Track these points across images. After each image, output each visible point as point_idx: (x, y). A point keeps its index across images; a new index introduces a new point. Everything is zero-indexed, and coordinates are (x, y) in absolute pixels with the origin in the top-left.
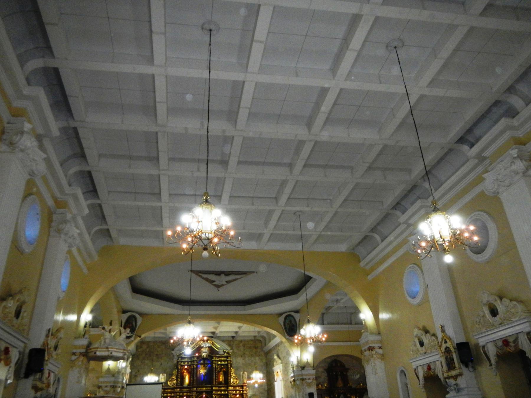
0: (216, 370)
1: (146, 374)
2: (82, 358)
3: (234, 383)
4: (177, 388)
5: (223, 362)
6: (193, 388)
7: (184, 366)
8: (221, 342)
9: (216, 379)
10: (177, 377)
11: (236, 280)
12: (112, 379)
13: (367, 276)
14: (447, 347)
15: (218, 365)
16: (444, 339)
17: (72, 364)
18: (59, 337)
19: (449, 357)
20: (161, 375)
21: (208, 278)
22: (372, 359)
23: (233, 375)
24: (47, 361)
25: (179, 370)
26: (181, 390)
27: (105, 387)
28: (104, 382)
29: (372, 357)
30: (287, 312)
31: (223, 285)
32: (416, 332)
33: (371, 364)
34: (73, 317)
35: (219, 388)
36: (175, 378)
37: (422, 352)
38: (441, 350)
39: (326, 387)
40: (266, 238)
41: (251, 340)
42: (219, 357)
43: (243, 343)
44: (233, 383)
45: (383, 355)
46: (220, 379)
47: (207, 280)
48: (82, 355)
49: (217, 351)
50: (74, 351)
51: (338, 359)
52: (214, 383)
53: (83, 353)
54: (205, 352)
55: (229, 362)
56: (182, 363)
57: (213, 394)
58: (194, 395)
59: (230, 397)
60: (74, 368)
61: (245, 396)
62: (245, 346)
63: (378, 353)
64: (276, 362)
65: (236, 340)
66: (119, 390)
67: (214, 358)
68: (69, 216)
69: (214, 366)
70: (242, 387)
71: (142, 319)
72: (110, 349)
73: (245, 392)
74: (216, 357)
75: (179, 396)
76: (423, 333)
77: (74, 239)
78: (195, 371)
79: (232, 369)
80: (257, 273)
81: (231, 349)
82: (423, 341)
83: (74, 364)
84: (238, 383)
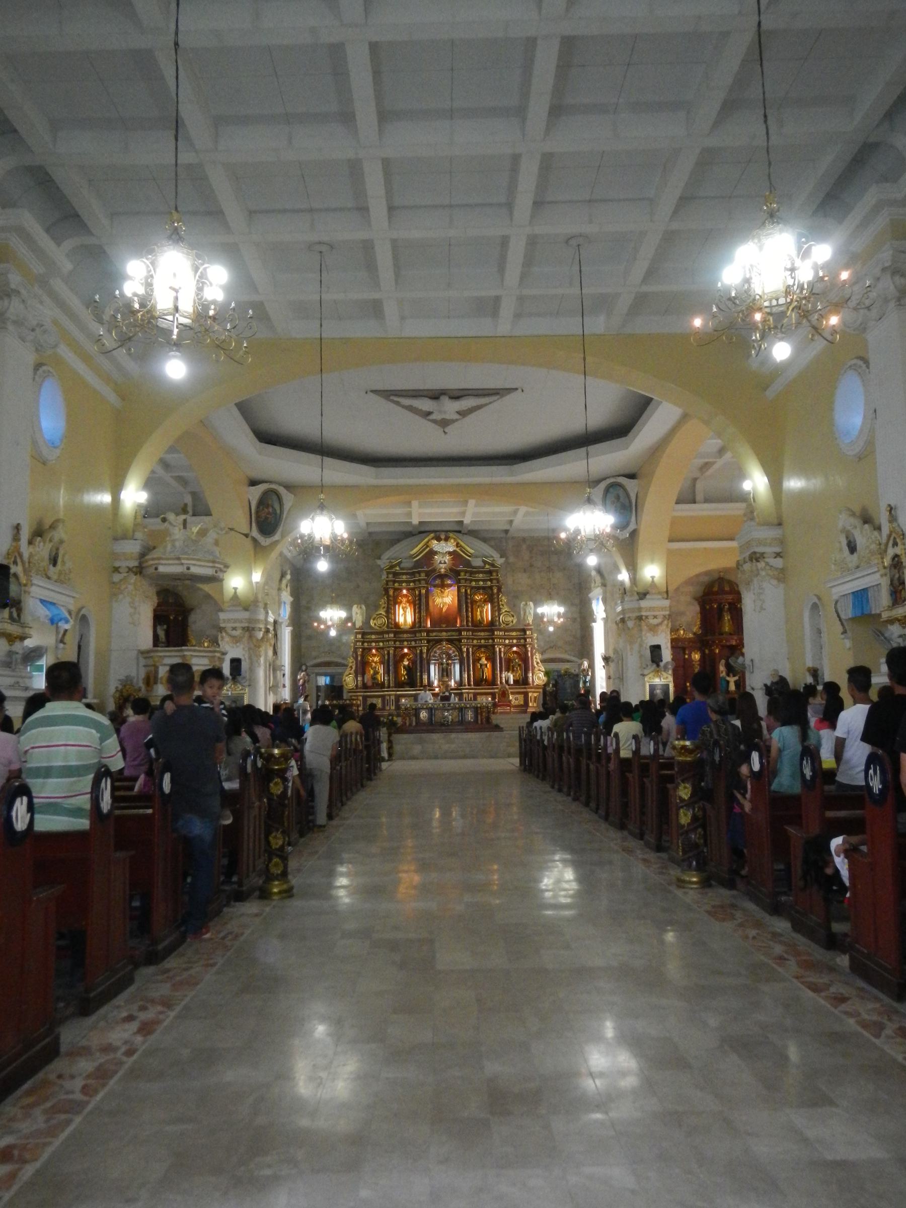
0: (466, 598)
1: (323, 607)
2: (133, 578)
3: (507, 625)
4: (388, 633)
5: (481, 583)
6: (420, 631)
7: (401, 590)
8: (483, 544)
9: (467, 617)
10: (388, 612)
11: (479, 407)
12: (246, 615)
13: (765, 391)
14: (896, 556)
15: (472, 588)
16: (892, 538)
17: (115, 591)
18: (56, 539)
19: (897, 576)
20: (355, 606)
21: (415, 405)
22: (755, 580)
23: (505, 609)
24: (25, 585)
25: (391, 599)
26: (397, 636)
27: (232, 630)
28: (229, 621)
29: (758, 575)
30: (608, 478)
31: (453, 421)
32: (844, 521)
33: (754, 590)
34: (105, 498)
35: (474, 634)
36: (384, 613)
37: (850, 565)
38: (883, 562)
39: (694, 634)
40: (507, 308)
42: (471, 573)
44: (504, 623)
45: (783, 570)
46: (477, 615)
47: (410, 409)
48: (133, 572)
49: (468, 560)
50: (117, 564)
51: (727, 577)
52: (465, 623)
53: (133, 567)
54: (442, 562)
55: (494, 581)
56: (396, 585)
57: (463, 645)
60: (121, 596)
61: (529, 649)
63: (772, 566)
64: (595, 582)
65: (513, 538)
66: (260, 635)
67: (462, 574)
68: (15, 279)
70: (524, 631)
71: (293, 496)
72: (183, 561)
74: (466, 572)
75: (393, 647)
76: (857, 522)
77: (45, 332)
78: (423, 600)
79: (502, 596)
80: (523, 391)
81: (501, 557)
82: (855, 541)
83: (119, 589)
84: (516, 622)
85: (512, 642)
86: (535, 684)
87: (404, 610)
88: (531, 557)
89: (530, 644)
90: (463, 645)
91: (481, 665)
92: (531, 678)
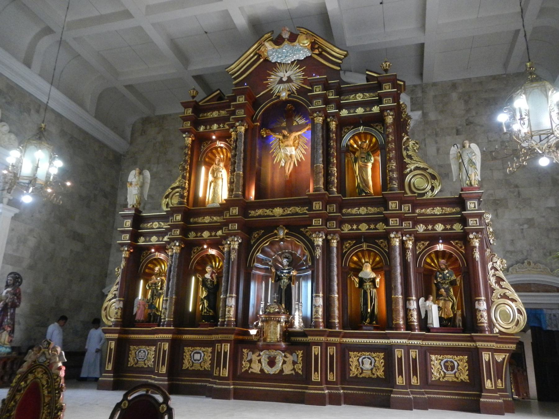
26: (192, 220)
35: (344, 211)
41: (494, 78)
43: (460, 90)
54: (285, 79)
56: (202, 129)
57: (314, 231)
59: (396, 243)
61: (476, 243)
62: (470, 97)
65: (434, 84)
70: (461, 202)
73: (472, 222)
75: (177, 239)
85: (433, 229)
86: (496, 330)
87: (213, 176)
88: (468, 111)
89: (478, 231)
91: (362, 281)
92: (485, 314)
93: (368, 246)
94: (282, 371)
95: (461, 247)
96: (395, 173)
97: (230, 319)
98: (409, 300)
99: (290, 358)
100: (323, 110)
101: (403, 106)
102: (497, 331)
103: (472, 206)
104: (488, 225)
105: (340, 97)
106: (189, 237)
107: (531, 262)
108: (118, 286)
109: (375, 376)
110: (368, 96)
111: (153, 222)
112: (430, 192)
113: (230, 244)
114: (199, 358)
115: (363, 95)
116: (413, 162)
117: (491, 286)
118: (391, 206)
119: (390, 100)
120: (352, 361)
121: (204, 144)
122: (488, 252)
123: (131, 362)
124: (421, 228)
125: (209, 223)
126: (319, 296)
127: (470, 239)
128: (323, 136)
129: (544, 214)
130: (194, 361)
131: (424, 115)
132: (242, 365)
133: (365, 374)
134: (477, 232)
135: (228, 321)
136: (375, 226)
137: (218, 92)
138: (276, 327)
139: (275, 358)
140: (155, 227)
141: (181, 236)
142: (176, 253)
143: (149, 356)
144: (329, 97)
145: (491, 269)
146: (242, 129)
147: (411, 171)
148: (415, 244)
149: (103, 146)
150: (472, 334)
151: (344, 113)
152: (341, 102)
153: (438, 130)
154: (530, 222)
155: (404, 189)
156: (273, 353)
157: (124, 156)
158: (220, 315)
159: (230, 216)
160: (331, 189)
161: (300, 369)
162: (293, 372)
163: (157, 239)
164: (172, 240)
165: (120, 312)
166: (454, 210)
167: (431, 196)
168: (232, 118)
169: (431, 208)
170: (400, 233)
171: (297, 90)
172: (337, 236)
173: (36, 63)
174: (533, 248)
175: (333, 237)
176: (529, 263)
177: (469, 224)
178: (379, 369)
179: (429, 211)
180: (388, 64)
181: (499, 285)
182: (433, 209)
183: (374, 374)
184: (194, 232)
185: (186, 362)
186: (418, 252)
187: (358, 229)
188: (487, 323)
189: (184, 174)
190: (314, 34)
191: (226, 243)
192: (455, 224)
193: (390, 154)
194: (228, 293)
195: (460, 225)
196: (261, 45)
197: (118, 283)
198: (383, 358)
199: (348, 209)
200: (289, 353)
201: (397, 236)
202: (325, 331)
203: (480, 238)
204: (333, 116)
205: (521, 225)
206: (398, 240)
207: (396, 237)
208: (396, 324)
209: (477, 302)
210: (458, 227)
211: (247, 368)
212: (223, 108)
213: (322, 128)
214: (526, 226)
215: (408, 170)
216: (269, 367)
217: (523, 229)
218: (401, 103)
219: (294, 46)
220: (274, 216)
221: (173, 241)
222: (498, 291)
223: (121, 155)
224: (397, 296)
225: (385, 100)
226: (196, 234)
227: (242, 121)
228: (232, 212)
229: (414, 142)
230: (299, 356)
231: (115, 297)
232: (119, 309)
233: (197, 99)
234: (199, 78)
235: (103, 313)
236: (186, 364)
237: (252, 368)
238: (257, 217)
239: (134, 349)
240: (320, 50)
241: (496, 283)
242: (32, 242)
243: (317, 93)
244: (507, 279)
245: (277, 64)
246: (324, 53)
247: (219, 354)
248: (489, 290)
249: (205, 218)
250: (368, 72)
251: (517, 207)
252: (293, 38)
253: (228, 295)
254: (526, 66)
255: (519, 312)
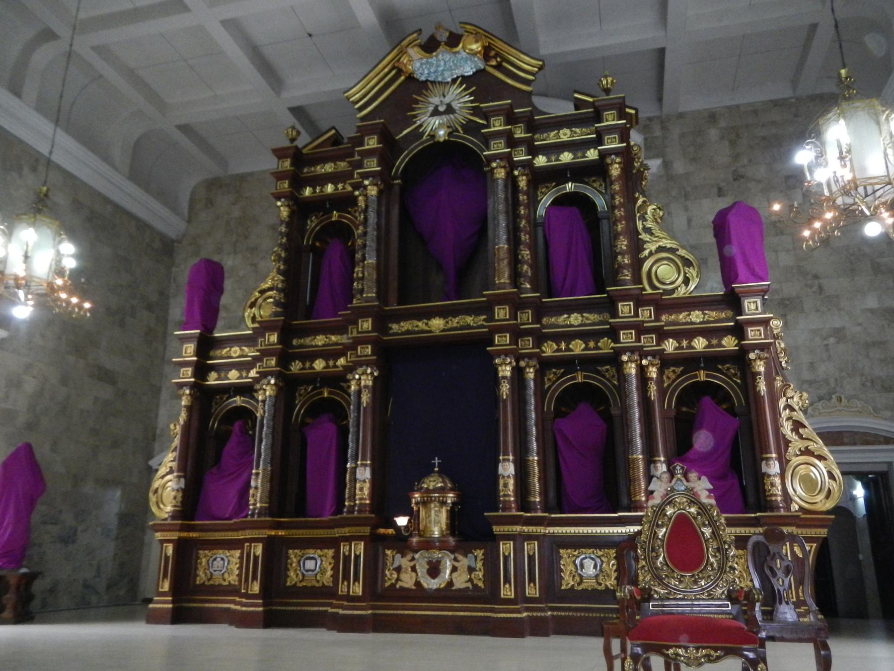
0: (514, 204)
26: (295, 342)
35: (545, 320)
41: (776, 103)
43: (723, 124)
54: (442, 109)
56: (308, 192)
57: (499, 354)
58: (360, 364)
59: (632, 369)
61: (760, 367)
62: (738, 136)
65: (681, 116)
69: (500, 174)
73: (754, 335)
75: (271, 374)
86: (795, 507)
89: (763, 347)
90: (499, 354)
92: (778, 481)
93: (585, 377)
94: (450, 583)
95: (735, 375)
96: (626, 256)
97: (363, 502)
98: (655, 462)
99: (464, 562)
100: (508, 157)
101: (635, 148)
102: (797, 507)
103: (753, 307)
104: (778, 339)
105: (534, 135)
106: (291, 370)
107: (843, 397)
108: (175, 454)
109: (602, 587)
110: (579, 134)
111: (231, 347)
112: (684, 287)
113: (360, 379)
114: (313, 568)
115: (571, 131)
116: (655, 239)
117: (784, 436)
118: (622, 311)
119: (615, 138)
120: (564, 565)
121: (312, 217)
122: (778, 383)
123: (201, 577)
124: (670, 346)
125: (324, 345)
126: (508, 460)
127: (750, 360)
128: (506, 199)
129: (860, 321)
130: (305, 573)
131: (666, 165)
132: (386, 576)
133: (586, 584)
134: (762, 350)
135: (361, 504)
136: (596, 344)
137: (333, 131)
138: (440, 512)
139: (439, 562)
140: (234, 355)
141: (278, 369)
142: (270, 396)
143: (231, 566)
144: (516, 136)
145: (785, 409)
146: (373, 191)
147: (651, 254)
148: (661, 372)
149: (142, 226)
150: (758, 514)
151: (541, 161)
152: (536, 143)
153: (688, 189)
154: (839, 334)
155: (641, 283)
156: (437, 555)
157: (179, 242)
158: (347, 496)
159: (359, 332)
160: (523, 286)
161: (480, 579)
162: (469, 585)
163: (238, 375)
164: (263, 375)
165: (180, 495)
166: (723, 315)
167: (684, 294)
168: (358, 173)
169: (687, 313)
170: (637, 353)
171: (462, 126)
172: (533, 362)
173: (31, 89)
174: (844, 374)
175: (528, 363)
176: (840, 400)
177: (748, 336)
178: (608, 576)
179: (682, 317)
180: (609, 79)
181: (798, 433)
182: (689, 315)
183: (600, 584)
184: (300, 361)
185: (292, 574)
186: (666, 385)
187: (568, 349)
188: (780, 496)
189: (279, 266)
190: (488, 34)
191: (354, 378)
192: (726, 336)
193: (617, 226)
194: (360, 459)
195: (734, 338)
196: (402, 52)
197: (176, 447)
198: (615, 558)
199: (552, 317)
200: (462, 554)
201: (632, 358)
202: (521, 516)
203: (766, 358)
204: (524, 167)
205: (825, 339)
206: (633, 365)
207: (630, 361)
208: (636, 501)
209: (764, 462)
210: (729, 343)
211: (393, 581)
212: (342, 159)
213: (506, 186)
214: (832, 340)
215: (646, 253)
216: (429, 578)
217: (827, 345)
218: (632, 143)
219: (455, 53)
220: (430, 332)
221: (265, 377)
222: (796, 444)
223: (173, 241)
224: (635, 456)
225: (608, 139)
226: (304, 364)
227: (373, 177)
228: (362, 326)
229: (655, 207)
230: (478, 559)
231: (171, 471)
232: (178, 490)
233: (300, 143)
234: (298, 112)
235: (153, 498)
236: (293, 578)
237: (401, 581)
238: (403, 334)
239: (206, 556)
240: (499, 59)
241: (792, 430)
242: (30, 385)
243: (496, 129)
244: (810, 424)
245: (429, 83)
246: (504, 64)
247: (347, 559)
248: (783, 444)
249: (318, 337)
250: (576, 95)
251: (818, 311)
252: (454, 40)
253: (359, 463)
254: (839, 75)
255: (831, 476)
